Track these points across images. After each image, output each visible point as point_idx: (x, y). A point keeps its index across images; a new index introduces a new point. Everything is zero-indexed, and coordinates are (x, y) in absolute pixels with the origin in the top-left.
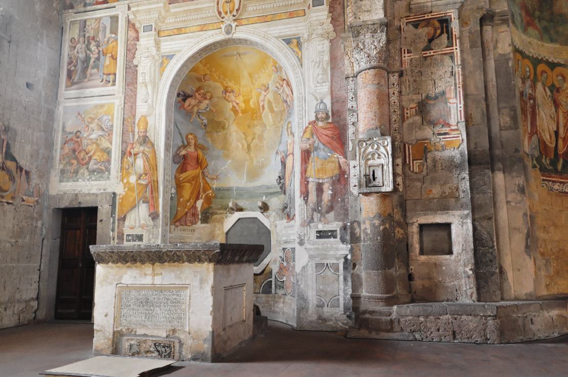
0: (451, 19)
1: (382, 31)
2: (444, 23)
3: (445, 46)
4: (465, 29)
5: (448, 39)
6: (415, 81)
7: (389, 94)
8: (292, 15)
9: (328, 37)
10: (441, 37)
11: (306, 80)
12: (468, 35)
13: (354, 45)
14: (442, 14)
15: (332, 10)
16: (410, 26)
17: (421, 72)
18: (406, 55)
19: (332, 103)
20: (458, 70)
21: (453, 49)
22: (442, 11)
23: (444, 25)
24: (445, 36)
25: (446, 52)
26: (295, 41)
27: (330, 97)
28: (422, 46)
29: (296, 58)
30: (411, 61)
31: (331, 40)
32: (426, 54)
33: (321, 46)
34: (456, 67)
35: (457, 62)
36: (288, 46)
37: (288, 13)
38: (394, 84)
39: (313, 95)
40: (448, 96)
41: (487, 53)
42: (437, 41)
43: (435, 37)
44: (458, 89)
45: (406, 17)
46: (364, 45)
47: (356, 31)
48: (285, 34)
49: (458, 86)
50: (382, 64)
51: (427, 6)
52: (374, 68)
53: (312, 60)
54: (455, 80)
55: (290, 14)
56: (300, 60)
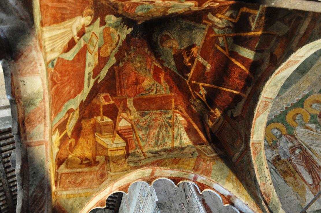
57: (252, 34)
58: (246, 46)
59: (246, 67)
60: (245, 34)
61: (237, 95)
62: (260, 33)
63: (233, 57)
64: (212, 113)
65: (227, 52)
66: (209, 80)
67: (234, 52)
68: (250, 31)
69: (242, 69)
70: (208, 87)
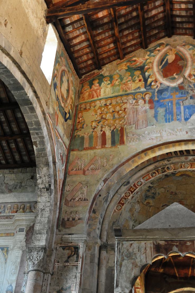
0: (80, 247)
1: (42, 252)
2: (76, 248)
3: (75, 261)
5: (77, 258)
6: (58, 279)
7: (42, 286)
8: (8, 235)
9: (22, 249)
11: (6, 271)
12: (90, 255)
13: (28, 257)
15: (27, 235)
16: (61, 248)
17: (61, 274)
18: (57, 264)
19: (16, 287)
20: (79, 275)
21: (78, 264)
23: (76, 250)
24: (75, 256)
25: (75, 264)
26: (6, 249)
27: (15, 283)
28: (65, 259)
29: (4, 259)
30: (58, 267)
31: (23, 251)
32: (66, 264)
33: (18, 253)
34: (78, 273)
35: (79, 270)
36: (1, 252)
37: (6, 234)
38: (46, 280)
39: (7, 281)
40: (72, 289)
41: (101, 265)
42: (71, 258)
44: (77, 286)
45: (60, 243)
46: (33, 257)
47: (35, 248)
48: (3, 244)
49: (77, 284)
50: (40, 269)
51: (69, 239)
52: (35, 270)
53: (12, 260)
54: (76, 280)
55: (7, 234)
56: (6, 260)
59: (191, 275)
61: (176, 276)
64: (159, 268)
69: (189, 273)
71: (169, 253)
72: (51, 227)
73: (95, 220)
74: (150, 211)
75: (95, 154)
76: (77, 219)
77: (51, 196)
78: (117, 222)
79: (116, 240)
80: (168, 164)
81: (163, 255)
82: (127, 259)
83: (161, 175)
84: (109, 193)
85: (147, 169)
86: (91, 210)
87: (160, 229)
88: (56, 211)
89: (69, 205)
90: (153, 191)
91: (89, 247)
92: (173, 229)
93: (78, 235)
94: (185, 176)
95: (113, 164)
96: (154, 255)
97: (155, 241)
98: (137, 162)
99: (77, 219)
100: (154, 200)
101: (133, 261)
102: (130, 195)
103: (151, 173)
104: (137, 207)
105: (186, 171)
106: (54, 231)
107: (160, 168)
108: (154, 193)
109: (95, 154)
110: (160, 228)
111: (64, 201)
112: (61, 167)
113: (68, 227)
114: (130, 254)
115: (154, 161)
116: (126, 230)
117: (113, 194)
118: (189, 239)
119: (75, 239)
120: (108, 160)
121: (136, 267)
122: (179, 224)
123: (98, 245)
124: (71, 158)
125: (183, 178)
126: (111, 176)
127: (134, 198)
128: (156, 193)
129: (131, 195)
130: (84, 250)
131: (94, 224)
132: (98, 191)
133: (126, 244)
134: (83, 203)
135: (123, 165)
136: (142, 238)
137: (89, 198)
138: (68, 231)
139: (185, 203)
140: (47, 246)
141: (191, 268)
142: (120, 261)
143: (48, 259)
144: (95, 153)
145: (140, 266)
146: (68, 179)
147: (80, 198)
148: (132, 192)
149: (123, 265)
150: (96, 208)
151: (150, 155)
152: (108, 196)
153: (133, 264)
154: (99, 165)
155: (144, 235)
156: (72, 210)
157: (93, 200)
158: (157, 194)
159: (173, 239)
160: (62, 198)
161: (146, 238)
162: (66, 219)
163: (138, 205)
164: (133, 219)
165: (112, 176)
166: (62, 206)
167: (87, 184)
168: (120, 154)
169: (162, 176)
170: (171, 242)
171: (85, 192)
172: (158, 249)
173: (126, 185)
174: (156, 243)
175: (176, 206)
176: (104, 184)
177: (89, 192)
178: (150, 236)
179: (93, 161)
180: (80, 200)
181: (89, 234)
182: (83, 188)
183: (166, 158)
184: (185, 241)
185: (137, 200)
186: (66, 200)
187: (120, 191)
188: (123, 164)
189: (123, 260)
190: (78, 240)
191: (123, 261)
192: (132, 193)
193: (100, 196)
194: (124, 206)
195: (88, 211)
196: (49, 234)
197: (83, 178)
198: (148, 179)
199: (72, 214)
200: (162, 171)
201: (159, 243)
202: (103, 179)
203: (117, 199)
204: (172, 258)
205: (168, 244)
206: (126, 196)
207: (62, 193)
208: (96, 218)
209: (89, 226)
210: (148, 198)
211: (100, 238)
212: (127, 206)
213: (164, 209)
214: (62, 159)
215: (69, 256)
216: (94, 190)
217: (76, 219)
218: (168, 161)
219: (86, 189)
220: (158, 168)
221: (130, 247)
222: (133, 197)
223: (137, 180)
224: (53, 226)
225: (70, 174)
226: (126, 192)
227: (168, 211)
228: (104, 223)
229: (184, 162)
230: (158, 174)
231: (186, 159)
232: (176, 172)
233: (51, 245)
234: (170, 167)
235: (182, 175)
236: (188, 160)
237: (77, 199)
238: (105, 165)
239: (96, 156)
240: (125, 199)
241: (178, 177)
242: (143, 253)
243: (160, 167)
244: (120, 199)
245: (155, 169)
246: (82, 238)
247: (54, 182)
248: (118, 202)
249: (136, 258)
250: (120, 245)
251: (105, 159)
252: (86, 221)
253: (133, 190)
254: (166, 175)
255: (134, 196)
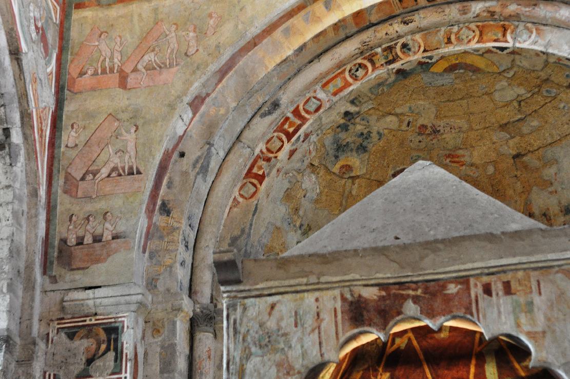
0: (123, 327)
2: (113, 331)
3: (110, 371)
4: (156, 340)
5: (116, 360)
10: (104, 356)
12: (159, 349)
14: (111, 318)
16: (63, 335)
22: (111, 313)
24: (111, 355)
42: (98, 363)
43: (96, 357)
51: (87, 305)
57: (517, 366)
58: (499, 367)
60: (512, 359)
62: (523, 374)
63: (477, 359)
64: (376, 371)
65: (479, 349)
66: (424, 343)
67: (484, 357)
68: (519, 363)
70: (414, 348)
71: (391, 323)
72: (22, 270)
73: (170, 237)
74: (354, 192)
75: (156, 14)
76: (107, 236)
77: (14, 168)
78: (245, 236)
79: (225, 295)
80: (406, 34)
81: (374, 330)
82: (260, 352)
83: (381, 72)
84: (211, 145)
85: (337, 56)
86: (155, 205)
87: (365, 250)
88: (36, 216)
89: (80, 194)
90: (359, 128)
91: (154, 324)
92: (405, 247)
93: (115, 288)
94: (462, 71)
95: (218, 47)
96: (343, 333)
97: (347, 289)
98: (302, 34)
99: (110, 237)
100: (366, 156)
101: (278, 357)
102: (282, 146)
103: (348, 67)
104: (310, 183)
105: (465, 52)
106: (35, 280)
107: (379, 50)
108: (362, 134)
109: (156, 14)
110: (366, 246)
111: (61, 181)
112: (40, 66)
113: (82, 266)
114: (269, 337)
115: (357, 24)
116: (255, 260)
117: (229, 146)
118: (454, 275)
119: (105, 301)
120: (201, 33)
121: (288, 373)
122: (427, 229)
123: (182, 314)
124: (74, 34)
125: (456, 78)
126: (217, 85)
127: (297, 156)
128: (370, 132)
129: (287, 147)
130: (140, 336)
131: (168, 251)
132: (175, 141)
133: (257, 307)
134: (126, 181)
135: (255, 45)
136: (306, 285)
137: (145, 166)
138: (82, 279)
139: (467, 159)
140: (15, 329)
141: (473, 362)
142: (238, 359)
143: (20, 371)
144: (156, 10)
145: (304, 371)
146: (69, 108)
147: (114, 169)
148: (289, 136)
149: (248, 371)
150: (171, 197)
151: (344, 8)
152: (208, 156)
153: (279, 365)
154: (172, 51)
155: (312, 273)
156: (89, 207)
157: (158, 170)
158: (374, 135)
159: (403, 280)
160: (55, 171)
161: (318, 283)
162: (72, 241)
163: (313, 177)
164: (298, 224)
165: (220, 86)
166: (56, 200)
167: (136, 120)
168: (241, 10)
169: (385, 76)
170: (399, 289)
171: (131, 146)
172: (357, 313)
173: (270, 113)
174: (352, 295)
175: (424, 173)
176: (194, 114)
177: (144, 145)
178: (331, 275)
179: (149, 39)
180: (114, 174)
181: (151, 284)
182: (121, 135)
183: (398, 12)
184: (441, 283)
185: (307, 162)
186: (68, 177)
187: (247, 134)
188: (254, 43)
189: (248, 356)
190: (117, 304)
191: (248, 358)
192: (289, 140)
193: (182, 155)
194: (264, 183)
195: (144, 207)
196: (20, 293)
197: (121, 99)
198: (341, 90)
199: (93, 223)
200: (387, 57)
201: (360, 296)
202: (188, 99)
203: (240, 161)
204: (416, 338)
205: (389, 295)
206: (269, 150)
207: (53, 152)
208: (174, 229)
209: (151, 257)
210: (343, 151)
211: (191, 292)
212: (274, 184)
213: (285, 192)
214: (43, 38)
215: (90, 357)
216: (161, 136)
217: (104, 239)
218: (406, 23)
219: (134, 135)
220: (372, 48)
221: (270, 314)
222: (292, 153)
223: (305, 95)
224: (29, 267)
225: (76, 89)
226: (270, 136)
227: (394, 190)
228: (202, 243)
229: (458, 23)
230: (373, 70)
231: (464, 12)
232: (433, 60)
233: (30, 327)
234: (410, 43)
235: (452, 68)
236: (470, 15)
237: (105, 172)
238: (192, 51)
239: (162, 20)
240: (268, 160)
241: (441, 75)
242: (309, 329)
243: (380, 46)
244: (252, 161)
245: (362, 53)
246: (127, 298)
247: (22, 118)
248: (245, 172)
249: (290, 347)
250: (235, 310)
251: (191, 28)
252: (140, 242)
253: (291, 130)
254: (400, 72)
255: (296, 149)
